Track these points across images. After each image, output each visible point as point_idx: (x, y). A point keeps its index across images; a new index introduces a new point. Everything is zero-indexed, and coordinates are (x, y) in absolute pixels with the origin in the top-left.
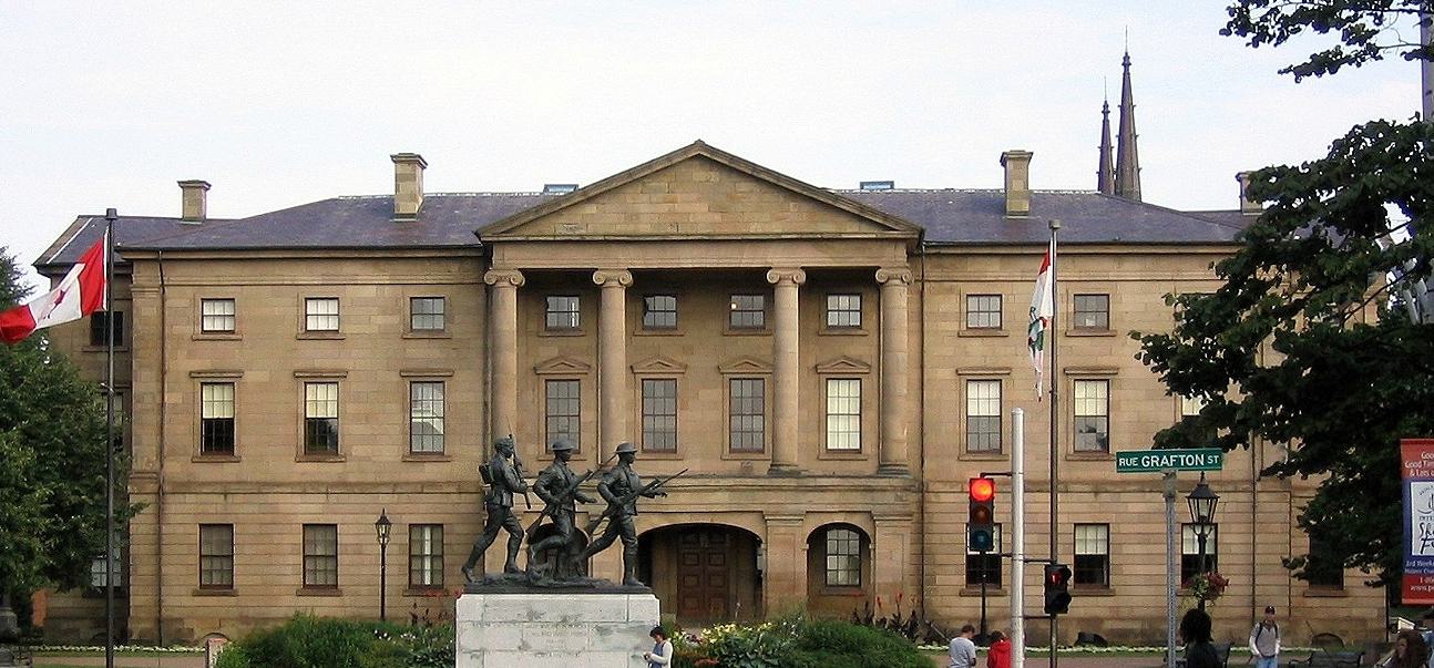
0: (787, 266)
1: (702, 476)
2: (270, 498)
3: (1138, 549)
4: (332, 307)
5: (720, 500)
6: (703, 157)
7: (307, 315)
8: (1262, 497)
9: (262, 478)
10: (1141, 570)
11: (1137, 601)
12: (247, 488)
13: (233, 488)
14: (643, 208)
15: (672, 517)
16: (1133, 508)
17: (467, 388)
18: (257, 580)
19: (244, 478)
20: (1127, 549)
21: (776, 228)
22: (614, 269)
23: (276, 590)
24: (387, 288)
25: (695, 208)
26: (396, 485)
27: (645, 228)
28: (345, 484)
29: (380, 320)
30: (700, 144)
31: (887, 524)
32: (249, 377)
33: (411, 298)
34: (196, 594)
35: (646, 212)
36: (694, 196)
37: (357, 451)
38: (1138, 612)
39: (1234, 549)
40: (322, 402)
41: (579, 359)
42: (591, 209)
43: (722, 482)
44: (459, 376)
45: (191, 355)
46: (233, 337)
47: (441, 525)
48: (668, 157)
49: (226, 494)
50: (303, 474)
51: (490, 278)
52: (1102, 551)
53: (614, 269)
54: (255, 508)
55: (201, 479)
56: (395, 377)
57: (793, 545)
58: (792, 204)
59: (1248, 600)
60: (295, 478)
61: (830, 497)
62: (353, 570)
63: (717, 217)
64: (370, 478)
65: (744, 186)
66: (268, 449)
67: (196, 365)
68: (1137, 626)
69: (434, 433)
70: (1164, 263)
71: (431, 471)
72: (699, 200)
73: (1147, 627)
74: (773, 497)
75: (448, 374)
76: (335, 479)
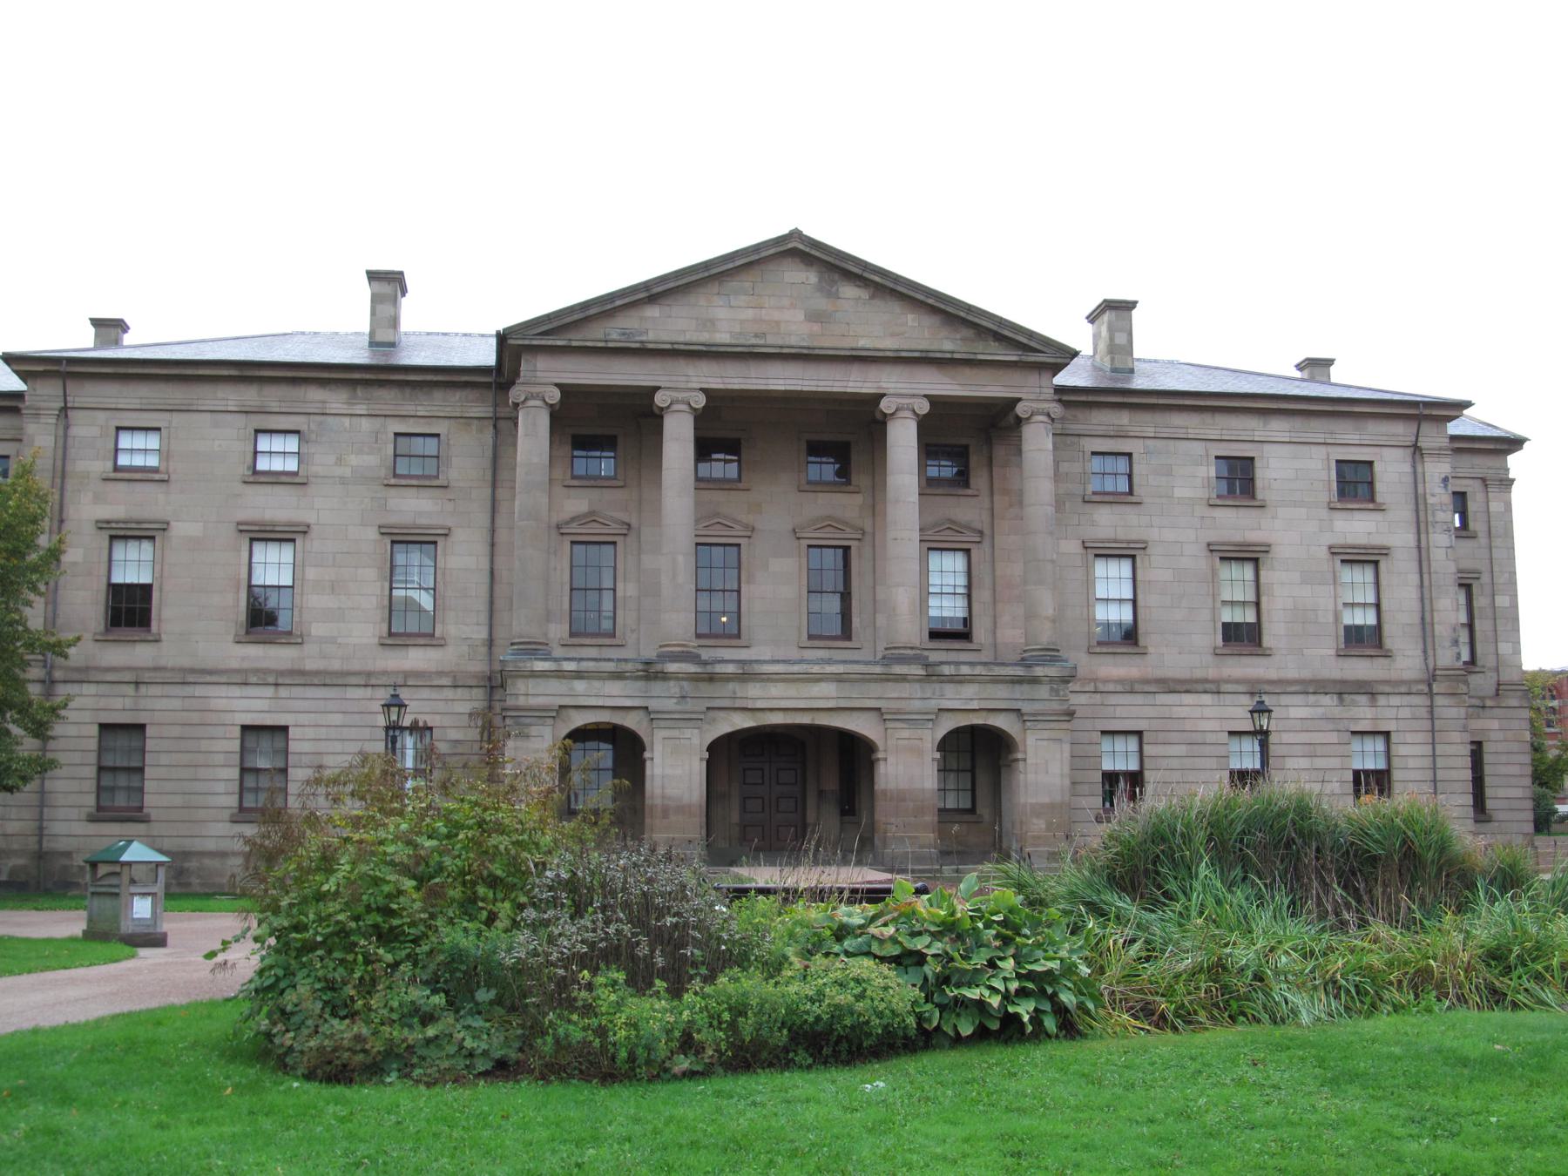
0: (906, 395)
1: (784, 662)
2: (199, 691)
3: (1303, 763)
4: (292, 444)
5: (825, 693)
6: (797, 251)
7: (256, 453)
8: (1439, 701)
9: (186, 662)
12: (168, 676)
13: (147, 677)
14: (722, 313)
15: (759, 714)
16: (1296, 713)
17: (464, 556)
18: (178, 800)
19: (162, 663)
21: (888, 344)
22: (681, 392)
23: (201, 814)
24: (364, 420)
25: (786, 311)
26: (369, 674)
27: (722, 337)
28: (302, 673)
29: (354, 460)
30: (796, 234)
31: (1040, 725)
32: (179, 529)
33: (396, 434)
34: (92, 819)
35: (725, 317)
36: (786, 302)
37: (317, 629)
39: (1411, 763)
40: (273, 567)
42: (653, 312)
43: (829, 669)
44: (459, 535)
45: (98, 499)
46: (157, 477)
49: (137, 683)
50: (243, 659)
51: (516, 394)
53: (681, 392)
54: (177, 704)
55: (104, 664)
56: (372, 534)
58: (910, 317)
60: (234, 664)
61: (970, 690)
63: (816, 328)
64: (336, 665)
65: (849, 291)
66: (196, 626)
67: (105, 512)
69: (420, 610)
70: (1316, 424)
71: (416, 659)
72: (793, 306)
74: (893, 690)
76: (288, 666)
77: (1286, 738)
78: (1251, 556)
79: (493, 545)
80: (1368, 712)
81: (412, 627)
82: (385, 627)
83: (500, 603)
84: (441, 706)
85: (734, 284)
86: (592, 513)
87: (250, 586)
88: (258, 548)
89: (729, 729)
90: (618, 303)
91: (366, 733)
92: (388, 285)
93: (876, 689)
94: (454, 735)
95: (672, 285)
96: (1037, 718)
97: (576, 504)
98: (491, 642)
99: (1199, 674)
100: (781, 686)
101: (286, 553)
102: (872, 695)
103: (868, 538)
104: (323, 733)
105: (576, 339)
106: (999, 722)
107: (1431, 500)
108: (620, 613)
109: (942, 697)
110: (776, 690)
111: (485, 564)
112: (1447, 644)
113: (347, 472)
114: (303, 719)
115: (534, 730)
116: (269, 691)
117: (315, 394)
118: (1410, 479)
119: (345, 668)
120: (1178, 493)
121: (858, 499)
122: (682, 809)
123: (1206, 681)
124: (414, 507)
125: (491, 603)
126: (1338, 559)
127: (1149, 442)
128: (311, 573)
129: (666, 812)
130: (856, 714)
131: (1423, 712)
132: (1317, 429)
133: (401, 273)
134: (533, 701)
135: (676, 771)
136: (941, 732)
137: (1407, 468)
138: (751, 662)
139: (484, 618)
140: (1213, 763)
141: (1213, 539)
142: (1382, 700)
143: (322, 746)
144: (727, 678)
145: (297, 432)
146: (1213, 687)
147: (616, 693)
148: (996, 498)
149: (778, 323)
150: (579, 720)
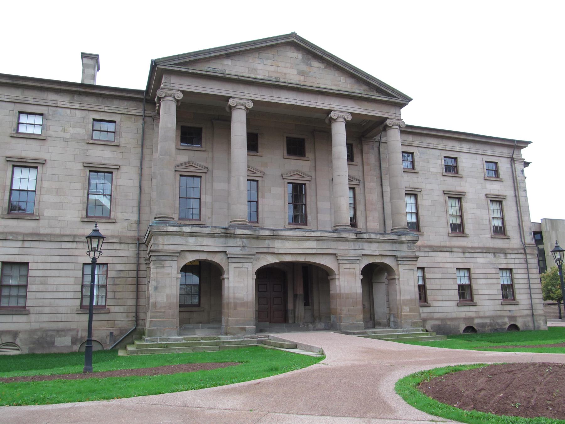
0: (342, 111)
3: (484, 281)
4: (39, 120)
5: (311, 246)
6: (294, 43)
8: (529, 257)
10: (486, 292)
11: (486, 308)
15: (280, 256)
17: (127, 179)
20: (480, 281)
22: (242, 99)
24: (77, 112)
26: (75, 236)
29: (71, 130)
30: (294, 35)
31: (405, 263)
33: (94, 120)
36: (288, 65)
37: (47, 213)
38: (487, 314)
41: (202, 164)
44: (124, 169)
47: (107, 264)
48: (277, 38)
50: (5, 227)
52: (467, 282)
53: (242, 99)
56: (80, 166)
57: (354, 275)
59: (528, 307)
61: (374, 246)
62: (40, 295)
63: (302, 78)
64: (57, 231)
65: (316, 64)
68: (488, 321)
72: (291, 67)
73: (492, 321)
74: (342, 245)
75: (118, 167)
77: (477, 271)
78: (458, 197)
79: (141, 175)
80: (504, 261)
81: (99, 214)
82: (84, 213)
83: (144, 203)
84: (113, 253)
85: (264, 55)
86: (190, 162)
87: (11, 190)
88: (17, 172)
89: (265, 263)
90: (212, 55)
91: (72, 266)
92: (91, 60)
93: (334, 245)
94: (119, 267)
95: (238, 50)
96: (404, 259)
97: (184, 157)
98: (139, 222)
99: (443, 244)
100: (290, 242)
101: (33, 174)
102: (332, 247)
103: (313, 181)
104: (48, 266)
105: (192, 69)
106: (387, 261)
107: (518, 178)
108: (203, 209)
109: (363, 249)
110: (289, 244)
111: (137, 184)
112: (528, 234)
113: (67, 136)
114: (37, 259)
115: (167, 263)
116: (19, 244)
117: (52, 97)
118: (510, 170)
119: (62, 233)
120: (432, 170)
121: (308, 164)
122: (244, 304)
123: (446, 247)
124: (102, 155)
125: (140, 202)
126: (489, 199)
127: (420, 149)
128: (46, 184)
129: (236, 306)
130: (324, 257)
131: (523, 261)
132: (478, 148)
133: (98, 55)
134: (167, 248)
135: (240, 285)
136: (363, 266)
137: (509, 166)
138: (277, 230)
139: (136, 209)
140: (451, 281)
141: (445, 189)
142: (509, 256)
143: (48, 273)
144: (265, 238)
145: (41, 115)
146: (450, 249)
147: (210, 244)
148: (365, 167)
149: (285, 74)
150: (190, 258)
